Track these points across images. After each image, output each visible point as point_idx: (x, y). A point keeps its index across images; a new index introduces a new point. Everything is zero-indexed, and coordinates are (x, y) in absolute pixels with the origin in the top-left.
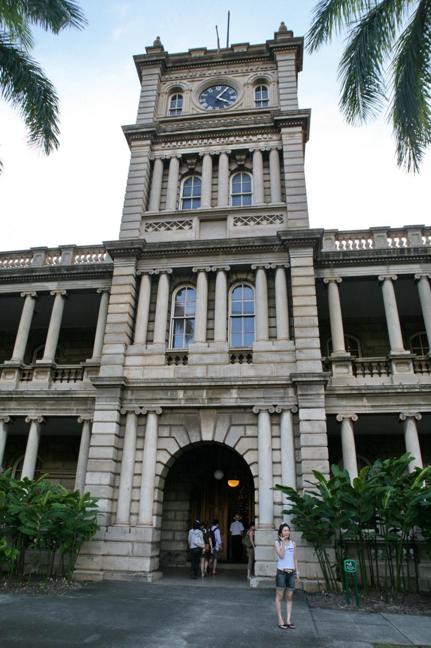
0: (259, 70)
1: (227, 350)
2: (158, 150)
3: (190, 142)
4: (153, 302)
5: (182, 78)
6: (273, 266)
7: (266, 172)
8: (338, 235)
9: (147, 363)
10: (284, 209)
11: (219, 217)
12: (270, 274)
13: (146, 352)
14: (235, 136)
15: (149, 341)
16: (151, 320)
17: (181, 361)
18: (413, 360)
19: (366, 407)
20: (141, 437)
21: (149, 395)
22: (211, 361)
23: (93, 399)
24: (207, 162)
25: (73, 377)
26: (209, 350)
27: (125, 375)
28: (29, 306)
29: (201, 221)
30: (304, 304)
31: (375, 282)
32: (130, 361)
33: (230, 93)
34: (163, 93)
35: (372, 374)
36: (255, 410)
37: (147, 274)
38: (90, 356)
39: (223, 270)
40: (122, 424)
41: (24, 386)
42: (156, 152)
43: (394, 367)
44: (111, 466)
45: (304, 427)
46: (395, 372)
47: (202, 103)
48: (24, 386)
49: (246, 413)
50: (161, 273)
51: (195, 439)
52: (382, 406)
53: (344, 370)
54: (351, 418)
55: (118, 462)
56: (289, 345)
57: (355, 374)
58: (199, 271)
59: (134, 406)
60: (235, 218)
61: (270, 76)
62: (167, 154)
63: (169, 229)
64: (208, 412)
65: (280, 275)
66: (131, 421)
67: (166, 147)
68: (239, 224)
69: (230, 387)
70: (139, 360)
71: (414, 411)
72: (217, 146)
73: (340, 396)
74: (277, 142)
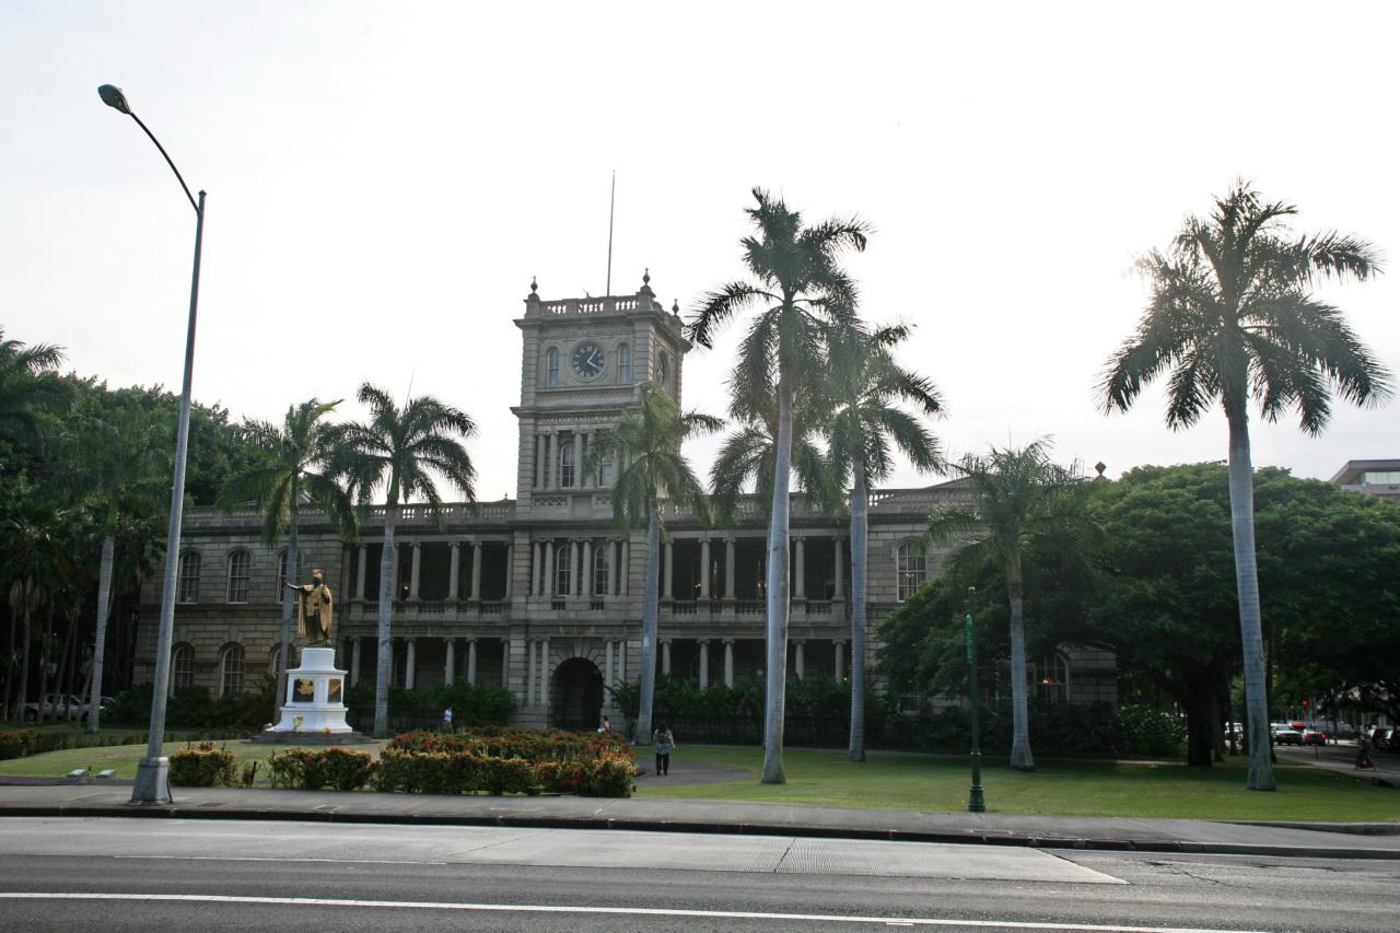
12: (619, 545)
16: (542, 573)
19: (678, 635)
20: (539, 655)
24: (578, 439)
28: (455, 553)
32: (530, 607)
33: (599, 355)
38: (504, 596)
40: (527, 647)
44: (524, 673)
45: (630, 652)
47: (575, 366)
49: (598, 643)
51: (571, 656)
53: (666, 610)
55: (527, 670)
62: (548, 428)
65: (625, 546)
69: (590, 626)
70: (535, 607)
71: (706, 638)
72: (585, 425)
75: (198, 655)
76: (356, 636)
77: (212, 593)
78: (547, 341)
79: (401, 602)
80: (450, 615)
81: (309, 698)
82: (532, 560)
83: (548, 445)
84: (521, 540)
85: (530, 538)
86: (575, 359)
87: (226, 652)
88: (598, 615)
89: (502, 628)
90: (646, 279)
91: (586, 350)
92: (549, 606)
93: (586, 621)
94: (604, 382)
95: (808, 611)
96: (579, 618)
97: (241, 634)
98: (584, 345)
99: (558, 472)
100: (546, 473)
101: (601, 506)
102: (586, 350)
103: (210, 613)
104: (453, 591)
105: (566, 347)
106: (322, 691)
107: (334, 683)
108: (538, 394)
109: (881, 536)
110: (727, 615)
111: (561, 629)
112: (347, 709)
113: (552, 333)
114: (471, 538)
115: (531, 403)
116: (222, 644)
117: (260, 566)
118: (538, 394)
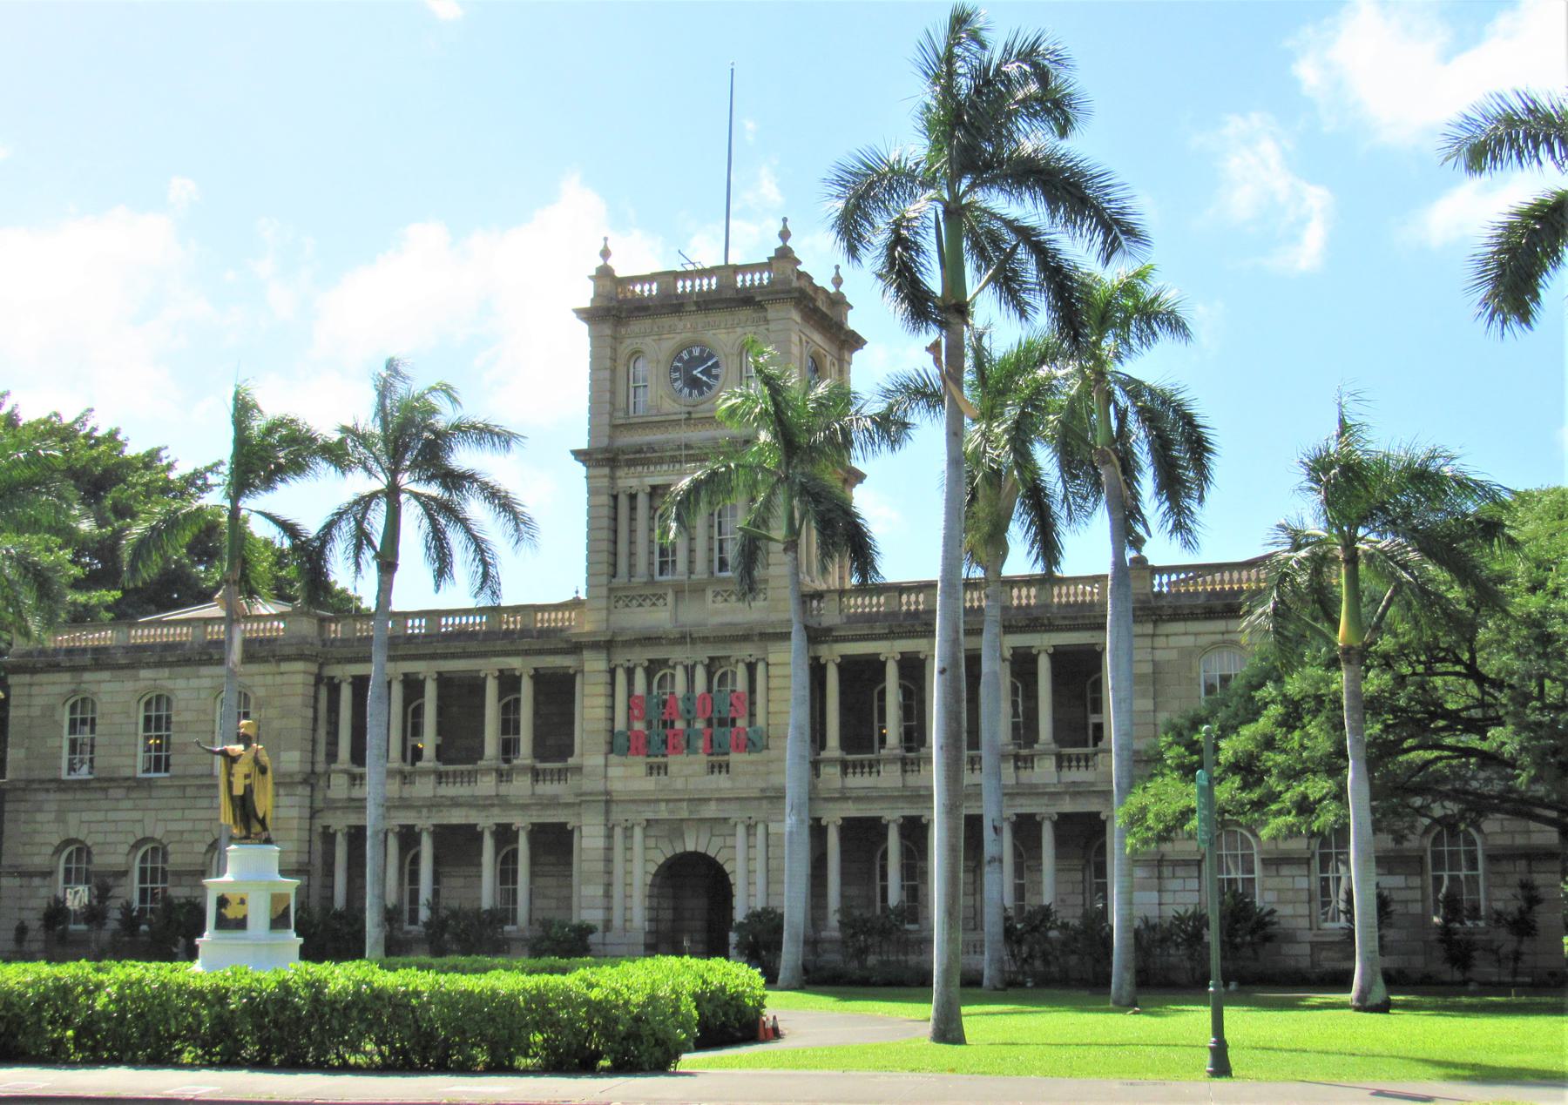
11: (698, 590)
12: (751, 668)
19: (853, 810)
20: (629, 849)
21: (633, 807)
36: (732, 822)
38: (571, 754)
40: (609, 836)
47: (676, 380)
48: (504, 789)
51: (679, 850)
55: (609, 873)
59: (622, 818)
65: (761, 668)
66: (618, 831)
69: (710, 799)
73: (827, 800)
75: (96, 860)
76: (339, 823)
77: (116, 761)
78: (628, 341)
79: (408, 768)
81: (241, 924)
82: (613, 695)
83: (633, 509)
85: (609, 661)
86: (676, 369)
87: (140, 854)
89: (568, 805)
90: (785, 235)
91: (690, 353)
93: (701, 791)
95: (1059, 766)
96: (691, 786)
97: (161, 826)
98: (688, 347)
99: (651, 553)
100: (632, 554)
101: (720, 605)
102: (690, 353)
103: (113, 793)
105: (658, 344)
106: (259, 914)
107: (276, 899)
108: (615, 427)
109: (1173, 641)
111: (663, 805)
112: (301, 940)
113: (637, 326)
114: (515, 663)
115: (605, 442)
116: (132, 841)
117: (187, 716)
118: (615, 427)
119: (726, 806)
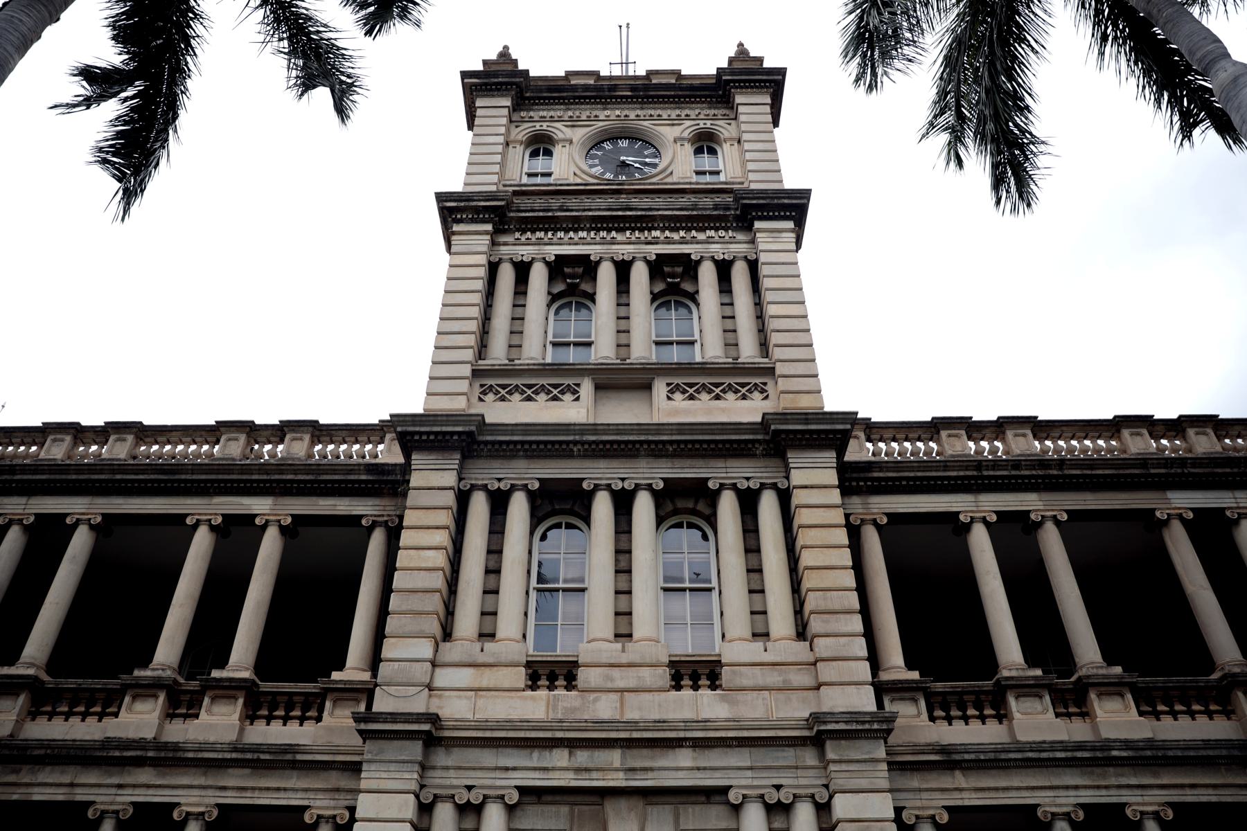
0: (701, 116)
1: (666, 660)
2: (506, 244)
3: (571, 234)
4: (495, 550)
5: (552, 119)
6: (754, 485)
7: (727, 300)
8: (874, 430)
9: (484, 684)
10: (770, 371)
12: (748, 502)
13: (481, 658)
14: (663, 230)
15: (487, 635)
16: (491, 591)
17: (561, 682)
18: (1052, 689)
22: (632, 684)
23: (355, 768)
24: (606, 274)
25: (297, 713)
26: (624, 659)
27: (433, 710)
28: (201, 545)
29: (599, 387)
30: (827, 563)
31: (955, 526)
32: (444, 678)
34: (515, 142)
35: (966, 719)
36: (733, 797)
37: (484, 488)
39: (649, 487)
41: (179, 732)
42: (502, 248)
43: (1012, 701)
46: (1017, 715)
47: (591, 166)
50: (513, 488)
52: (996, 789)
54: (933, 817)
56: (800, 650)
57: (932, 719)
58: (597, 488)
60: (668, 385)
61: (725, 130)
63: (529, 399)
64: (623, 803)
65: (768, 507)
67: (523, 239)
68: (678, 396)
70: (464, 677)
72: (624, 246)
74: (745, 246)
80: (139, 719)
84: (433, 478)
88: (704, 706)
92: (519, 676)
93: (660, 724)
94: (669, 180)
96: (632, 715)
98: (612, 136)
104: (168, 650)
110: (1116, 718)
119: (715, 758)
